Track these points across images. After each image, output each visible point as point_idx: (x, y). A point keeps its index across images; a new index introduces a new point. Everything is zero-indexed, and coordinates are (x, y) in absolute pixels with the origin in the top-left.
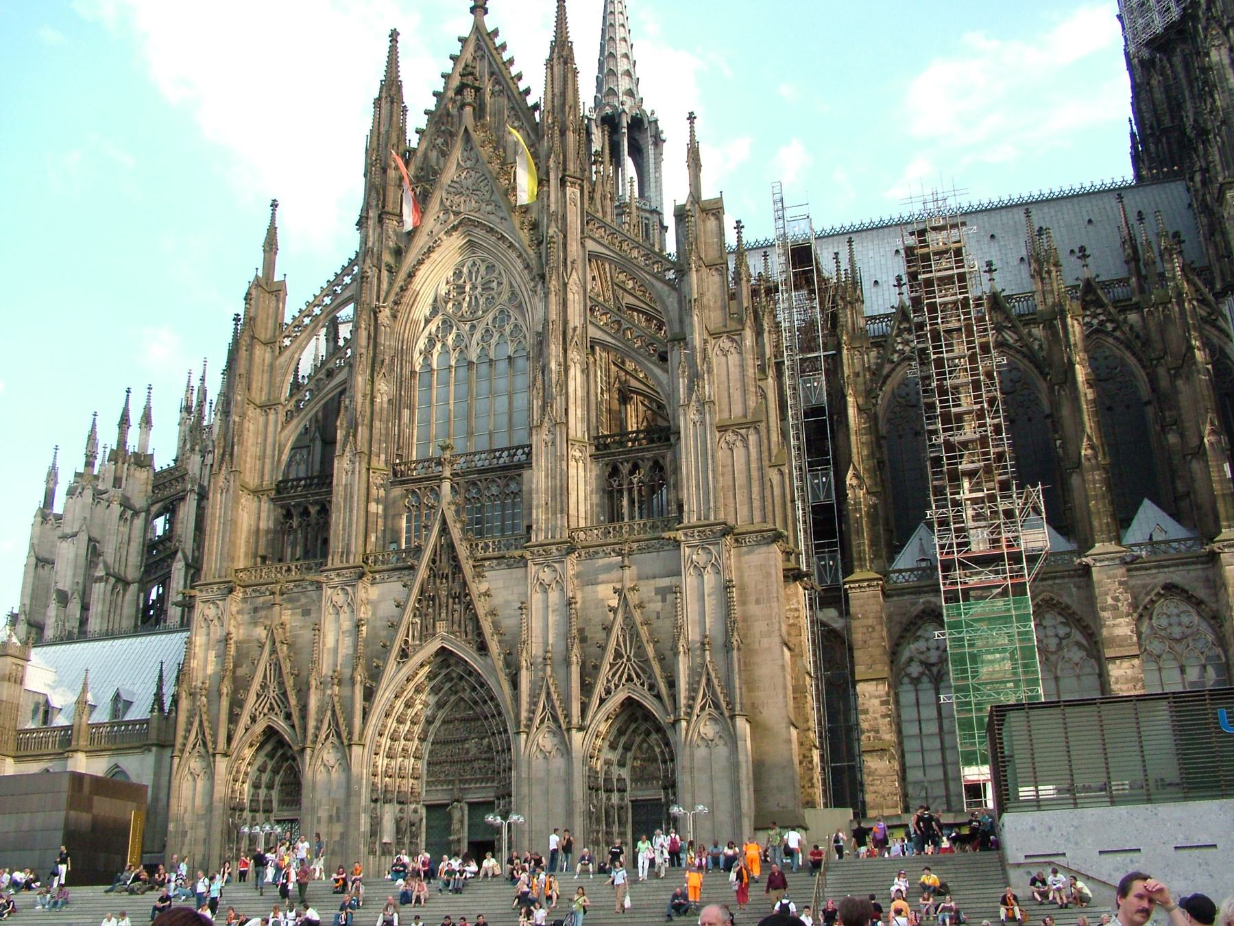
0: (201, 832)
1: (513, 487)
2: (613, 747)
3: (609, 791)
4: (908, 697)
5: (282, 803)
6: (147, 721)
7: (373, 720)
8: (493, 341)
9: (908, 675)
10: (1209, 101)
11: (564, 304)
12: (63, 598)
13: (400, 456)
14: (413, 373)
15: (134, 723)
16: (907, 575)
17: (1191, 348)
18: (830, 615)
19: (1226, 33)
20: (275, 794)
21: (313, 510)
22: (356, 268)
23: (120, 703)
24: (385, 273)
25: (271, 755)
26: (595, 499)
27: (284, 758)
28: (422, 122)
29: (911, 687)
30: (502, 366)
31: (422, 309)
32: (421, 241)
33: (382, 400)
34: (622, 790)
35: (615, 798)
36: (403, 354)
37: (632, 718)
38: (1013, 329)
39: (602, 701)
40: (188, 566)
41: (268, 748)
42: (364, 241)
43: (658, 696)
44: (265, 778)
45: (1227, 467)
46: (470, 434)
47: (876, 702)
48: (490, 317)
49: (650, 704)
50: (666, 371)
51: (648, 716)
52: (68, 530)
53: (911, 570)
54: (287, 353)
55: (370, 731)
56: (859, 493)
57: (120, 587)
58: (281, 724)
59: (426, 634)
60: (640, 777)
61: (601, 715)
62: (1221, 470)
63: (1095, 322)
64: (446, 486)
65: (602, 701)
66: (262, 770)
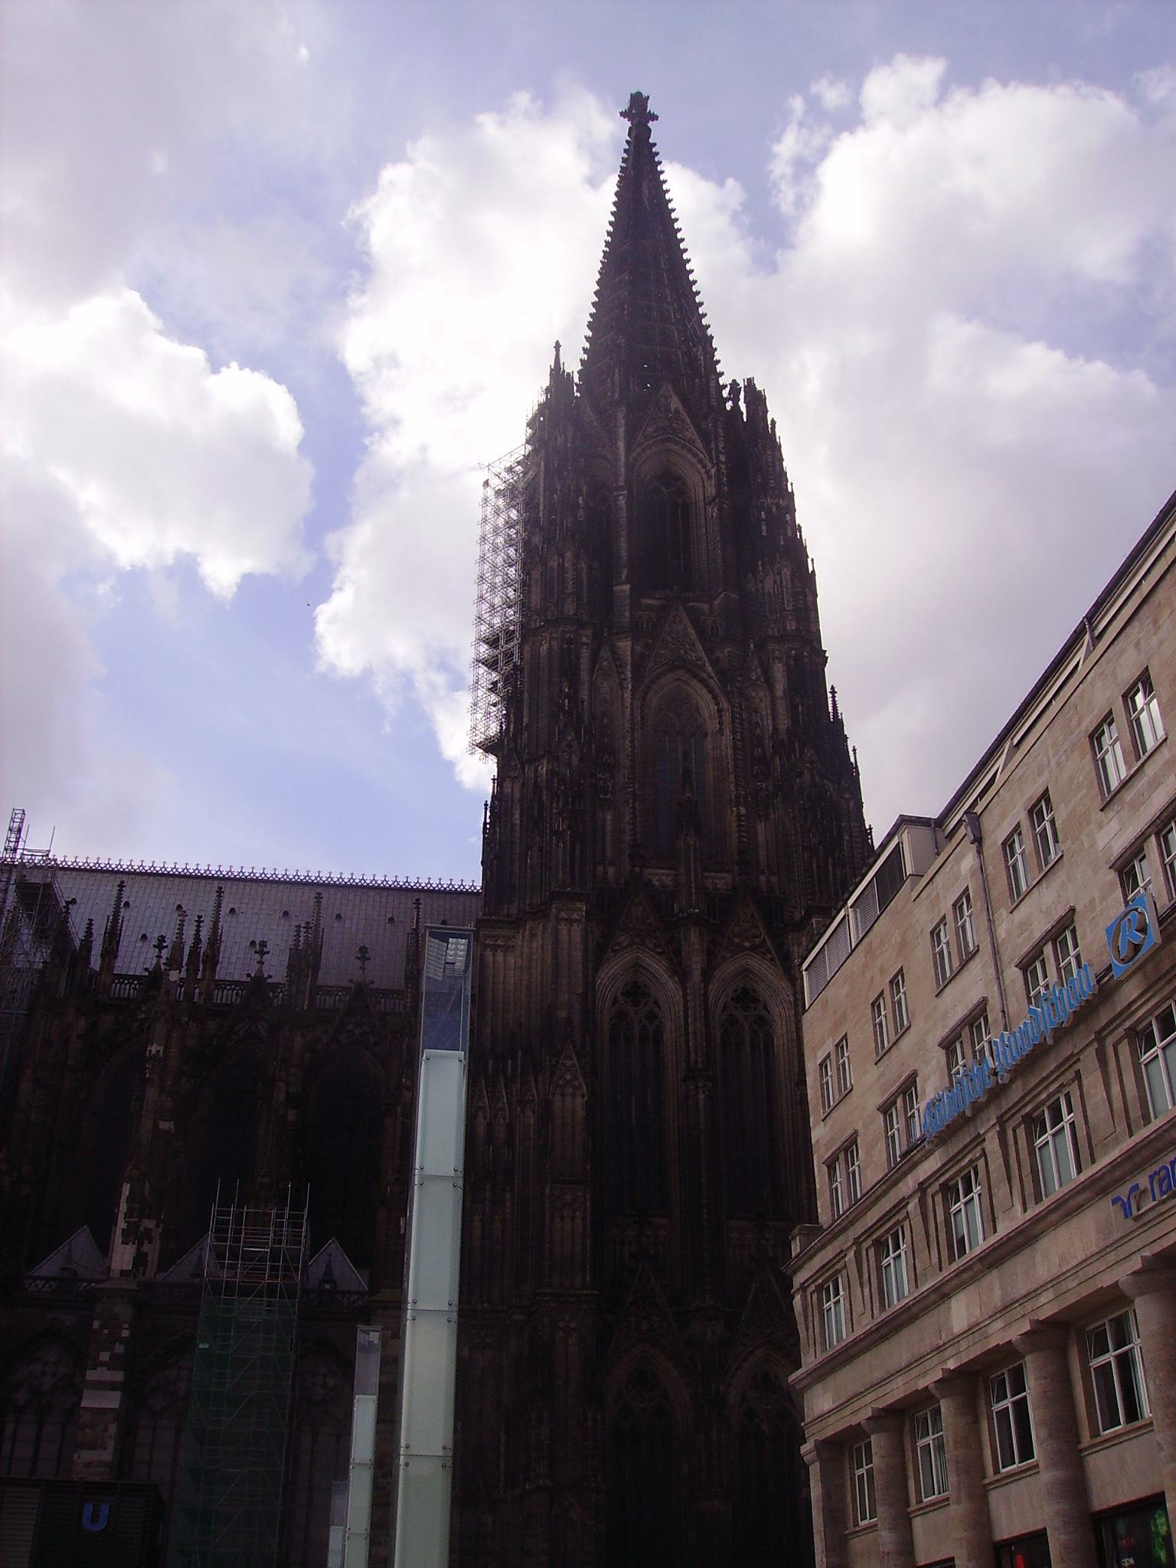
16: (40, 1283)
19: (523, 768)
53: (54, 1279)
63: (358, 1031)
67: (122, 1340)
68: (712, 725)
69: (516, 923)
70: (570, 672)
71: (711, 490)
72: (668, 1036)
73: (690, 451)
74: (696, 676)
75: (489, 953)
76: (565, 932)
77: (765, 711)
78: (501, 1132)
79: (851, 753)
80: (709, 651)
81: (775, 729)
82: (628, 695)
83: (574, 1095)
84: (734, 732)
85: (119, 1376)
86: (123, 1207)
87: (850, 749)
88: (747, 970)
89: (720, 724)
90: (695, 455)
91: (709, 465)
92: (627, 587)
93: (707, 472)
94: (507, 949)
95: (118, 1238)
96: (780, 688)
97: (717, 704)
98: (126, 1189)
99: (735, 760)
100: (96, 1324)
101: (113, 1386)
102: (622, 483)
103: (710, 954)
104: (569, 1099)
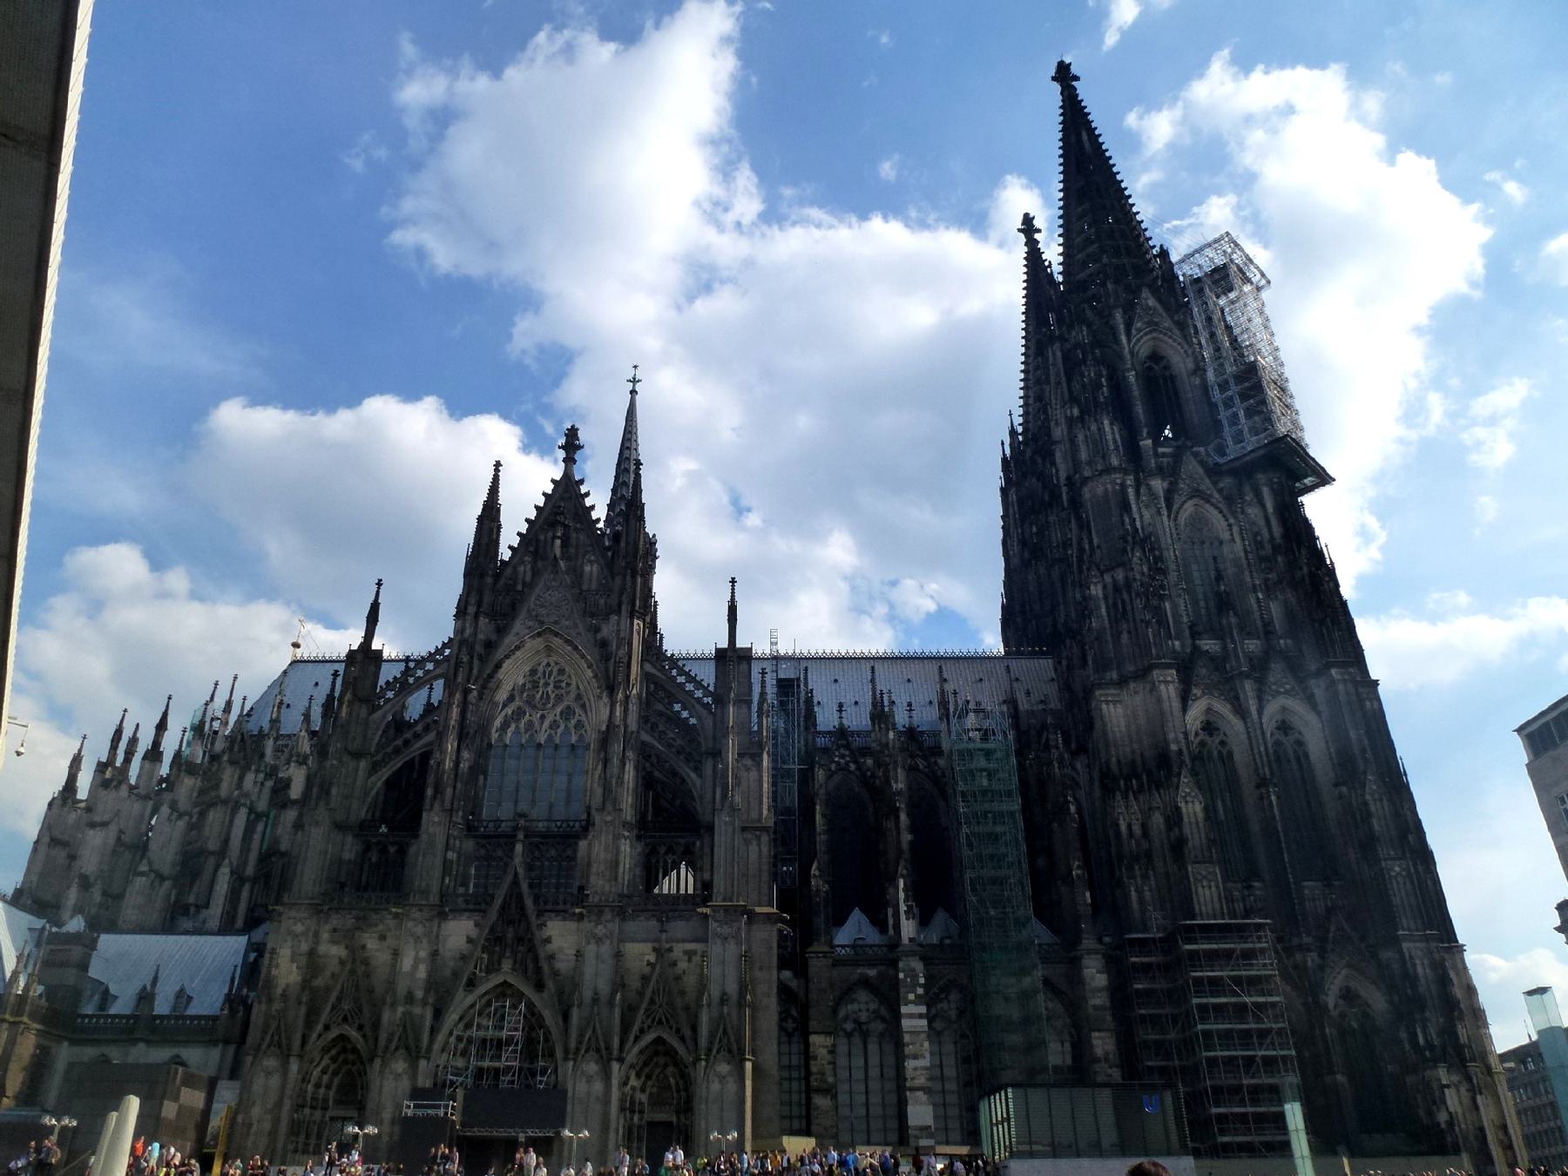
0: (267, 1126)
1: (569, 852)
2: (638, 1075)
3: (633, 1112)
4: (842, 1048)
5: (338, 1102)
6: (214, 1018)
7: (440, 1038)
8: (559, 731)
9: (844, 1030)
11: (626, 710)
12: (85, 883)
13: (472, 814)
14: (490, 745)
15: (200, 1017)
18: (787, 974)
20: (331, 1094)
21: (392, 850)
22: (447, 652)
23: (183, 997)
24: (476, 662)
25: (334, 1060)
26: (638, 871)
27: (345, 1062)
28: (515, 542)
29: (845, 1041)
30: (564, 751)
31: (501, 696)
32: (510, 640)
33: (464, 766)
34: (641, 1112)
35: (636, 1118)
36: (484, 729)
37: (656, 1053)
38: (925, 758)
39: (637, 1038)
40: (232, 873)
41: (334, 1052)
42: (459, 631)
43: (683, 1039)
44: (326, 1078)
45: (1088, 894)
46: (533, 802)
47: (823, 1051)
48: (558, 710)
49: (675, 1042)
50: (700, 776)
51: (671, 1053)
52: (97, 819)
54: (379, 713)
55: (437, 1046)
56: (818, 883)
57: (157, 883)
58: (353, 1033)
59: (492, 968)
60: (657, 1102)
61: (636, 1050)
64: (519, 848)
65: (637, 1038)
66: (324, 1072)
67: (921, 986)
68: (1226, 536)
69: (1122, 682)
70: (1126, 507)
72: (1240, 756)
74: (1208, 501)
75: (1104, 706)
77: (1262, 523)
78: (1137, 829)
80: (1215, 483)
81: (1272, 538)
82: (1165, 518)
84: (1243, 540)
85: (923, 1009)
86: (902, 895)
94: (1115, 702)
95: (903, 917)
98: (901, 883)
100: (901, 975)
101: (921, 1016)
102: (1129, 365)
103: (1260, 699)
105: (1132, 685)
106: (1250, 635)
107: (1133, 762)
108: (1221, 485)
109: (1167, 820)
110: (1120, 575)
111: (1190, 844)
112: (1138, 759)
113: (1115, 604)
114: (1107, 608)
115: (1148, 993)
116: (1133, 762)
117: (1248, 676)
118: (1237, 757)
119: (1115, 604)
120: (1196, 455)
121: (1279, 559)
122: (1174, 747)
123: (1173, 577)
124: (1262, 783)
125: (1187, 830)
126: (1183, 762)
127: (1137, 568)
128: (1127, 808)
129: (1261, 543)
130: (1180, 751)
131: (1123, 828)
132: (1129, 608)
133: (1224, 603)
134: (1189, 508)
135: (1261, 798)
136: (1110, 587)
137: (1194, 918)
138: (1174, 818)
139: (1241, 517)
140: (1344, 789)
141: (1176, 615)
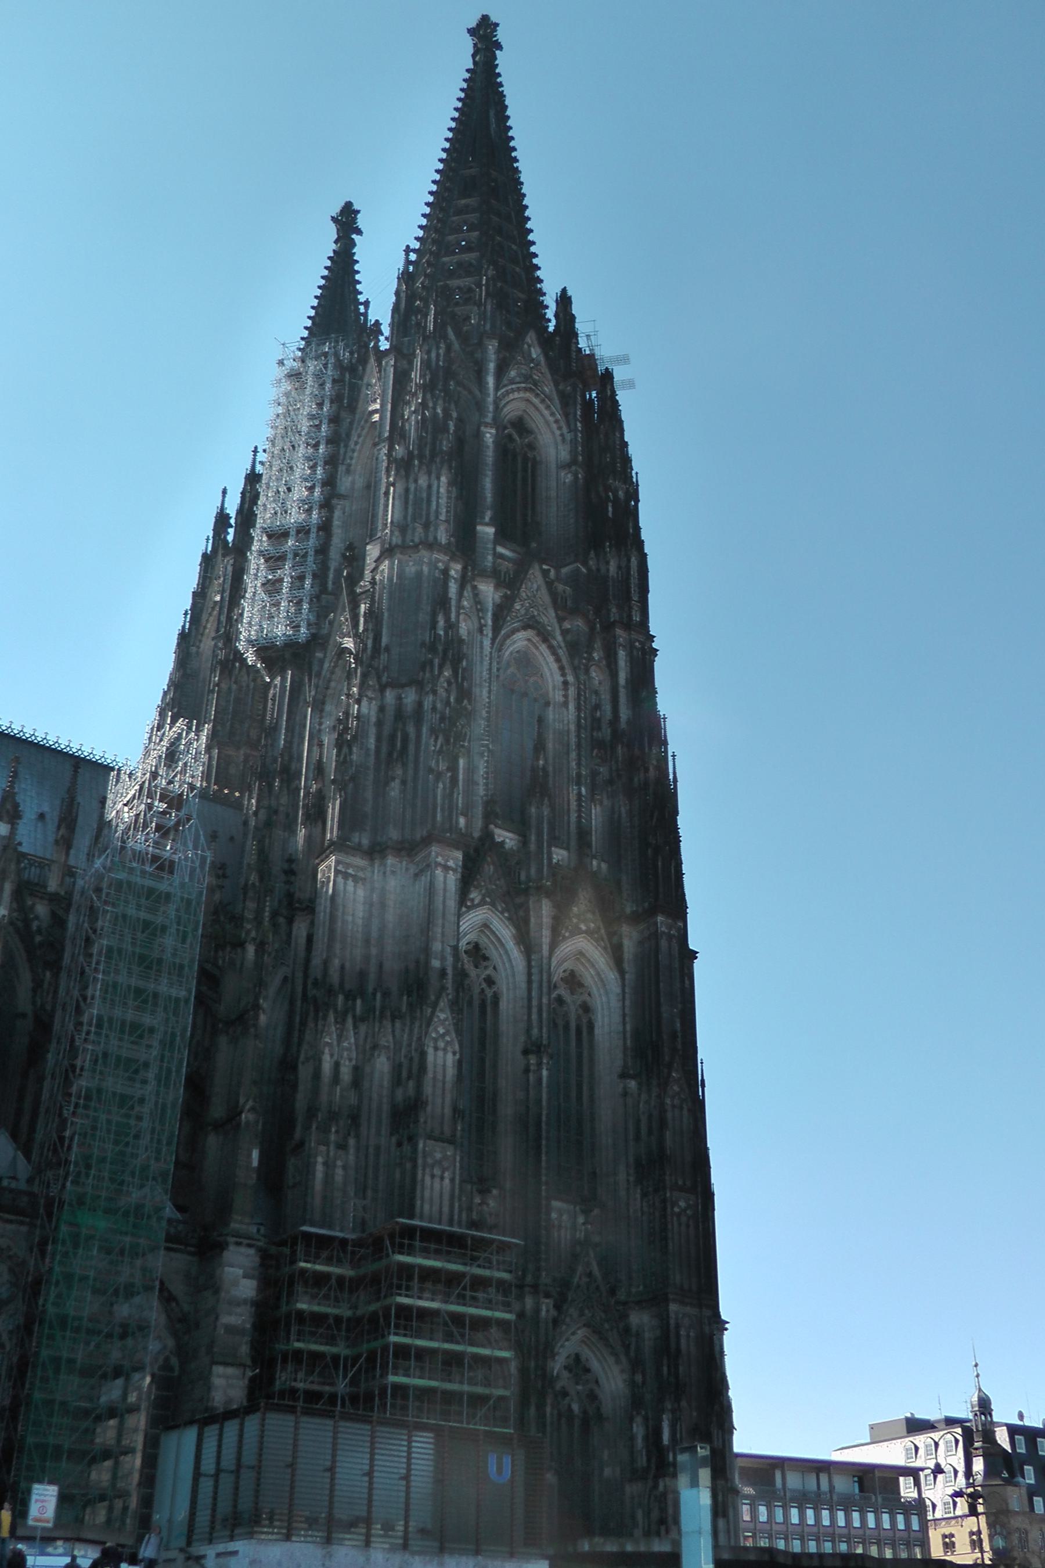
10: (345, 750)
17: (257, 1007)
19: (382, 689)
45: (255, 1154)
62: (250, 1155)
70: (442, 602)
71: (564, 455)
73: (548, 407)
74: (545, 640)
76: (441, 879)
77: (606, 697)
78: (346, 1073)
79: (670, 758)
80: (560, 620)
82: (487, 643)
83: (445, 1050)
84: (578, 709)
87: (670, 754)
88: (581, 953)
89: (566, 696)
90: (552, 414)
91: (565, 430)
92: (491, 530)
93: (562, 435)
94: (356, 879)
96: (622, 677)
97: (563, 675)
99: (578, 736)
102: (489, 419)
103: (555, 931)
104: (440, 1053)
105: (390, 861)
106: (555, 840)
107: (362, 975)
108: (567, 625)
109: (397, 1069)
110: (410, 697)
111: (429, 1108)
112: (373, 969)
113: (392, 737)
114: (379, 739)
115: (319, 1319)
116: (362, 975)
117: (549, 894)
118: (503, 1005)
119: (392, 737)
120: (545, 573)
121: (620, 750)
122: (436, 963)
123: (480, 726)
124: (533, 1048)
125: (428, 1089)
126: (443, 988)
127: (441, 692)
128: (340, 1037)
129: (599, 720)
130: (443, 973)
131: (327, 1066)
132: (411, 747)
133: (538, 785)
134: (520, 640)
135: (527, 1070)
136: (390, 712)
137: (411, 1216)
138: (411, 1069)
139: (582, 677)
140: (633, 1084)
141: (470, 782)
